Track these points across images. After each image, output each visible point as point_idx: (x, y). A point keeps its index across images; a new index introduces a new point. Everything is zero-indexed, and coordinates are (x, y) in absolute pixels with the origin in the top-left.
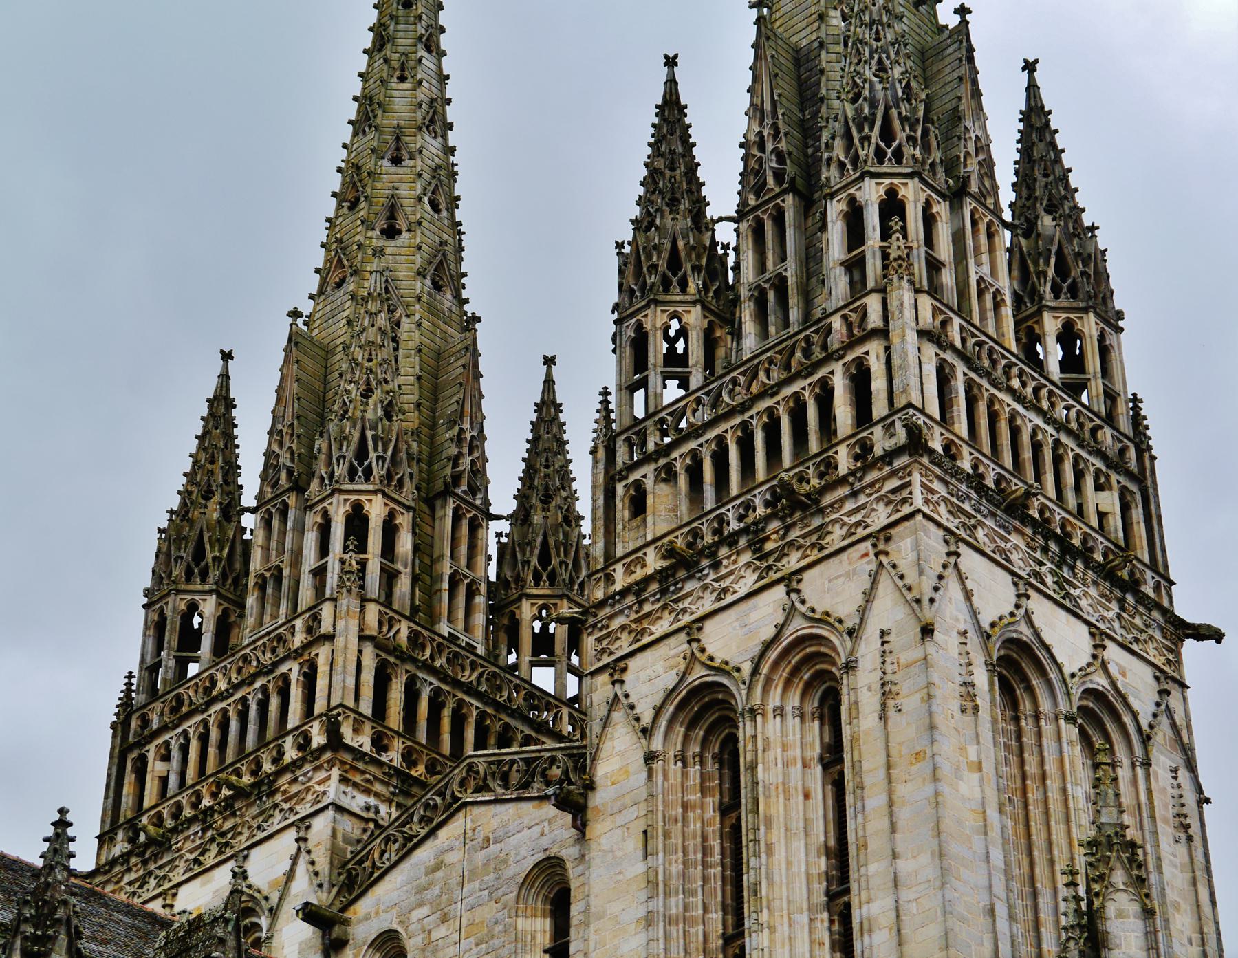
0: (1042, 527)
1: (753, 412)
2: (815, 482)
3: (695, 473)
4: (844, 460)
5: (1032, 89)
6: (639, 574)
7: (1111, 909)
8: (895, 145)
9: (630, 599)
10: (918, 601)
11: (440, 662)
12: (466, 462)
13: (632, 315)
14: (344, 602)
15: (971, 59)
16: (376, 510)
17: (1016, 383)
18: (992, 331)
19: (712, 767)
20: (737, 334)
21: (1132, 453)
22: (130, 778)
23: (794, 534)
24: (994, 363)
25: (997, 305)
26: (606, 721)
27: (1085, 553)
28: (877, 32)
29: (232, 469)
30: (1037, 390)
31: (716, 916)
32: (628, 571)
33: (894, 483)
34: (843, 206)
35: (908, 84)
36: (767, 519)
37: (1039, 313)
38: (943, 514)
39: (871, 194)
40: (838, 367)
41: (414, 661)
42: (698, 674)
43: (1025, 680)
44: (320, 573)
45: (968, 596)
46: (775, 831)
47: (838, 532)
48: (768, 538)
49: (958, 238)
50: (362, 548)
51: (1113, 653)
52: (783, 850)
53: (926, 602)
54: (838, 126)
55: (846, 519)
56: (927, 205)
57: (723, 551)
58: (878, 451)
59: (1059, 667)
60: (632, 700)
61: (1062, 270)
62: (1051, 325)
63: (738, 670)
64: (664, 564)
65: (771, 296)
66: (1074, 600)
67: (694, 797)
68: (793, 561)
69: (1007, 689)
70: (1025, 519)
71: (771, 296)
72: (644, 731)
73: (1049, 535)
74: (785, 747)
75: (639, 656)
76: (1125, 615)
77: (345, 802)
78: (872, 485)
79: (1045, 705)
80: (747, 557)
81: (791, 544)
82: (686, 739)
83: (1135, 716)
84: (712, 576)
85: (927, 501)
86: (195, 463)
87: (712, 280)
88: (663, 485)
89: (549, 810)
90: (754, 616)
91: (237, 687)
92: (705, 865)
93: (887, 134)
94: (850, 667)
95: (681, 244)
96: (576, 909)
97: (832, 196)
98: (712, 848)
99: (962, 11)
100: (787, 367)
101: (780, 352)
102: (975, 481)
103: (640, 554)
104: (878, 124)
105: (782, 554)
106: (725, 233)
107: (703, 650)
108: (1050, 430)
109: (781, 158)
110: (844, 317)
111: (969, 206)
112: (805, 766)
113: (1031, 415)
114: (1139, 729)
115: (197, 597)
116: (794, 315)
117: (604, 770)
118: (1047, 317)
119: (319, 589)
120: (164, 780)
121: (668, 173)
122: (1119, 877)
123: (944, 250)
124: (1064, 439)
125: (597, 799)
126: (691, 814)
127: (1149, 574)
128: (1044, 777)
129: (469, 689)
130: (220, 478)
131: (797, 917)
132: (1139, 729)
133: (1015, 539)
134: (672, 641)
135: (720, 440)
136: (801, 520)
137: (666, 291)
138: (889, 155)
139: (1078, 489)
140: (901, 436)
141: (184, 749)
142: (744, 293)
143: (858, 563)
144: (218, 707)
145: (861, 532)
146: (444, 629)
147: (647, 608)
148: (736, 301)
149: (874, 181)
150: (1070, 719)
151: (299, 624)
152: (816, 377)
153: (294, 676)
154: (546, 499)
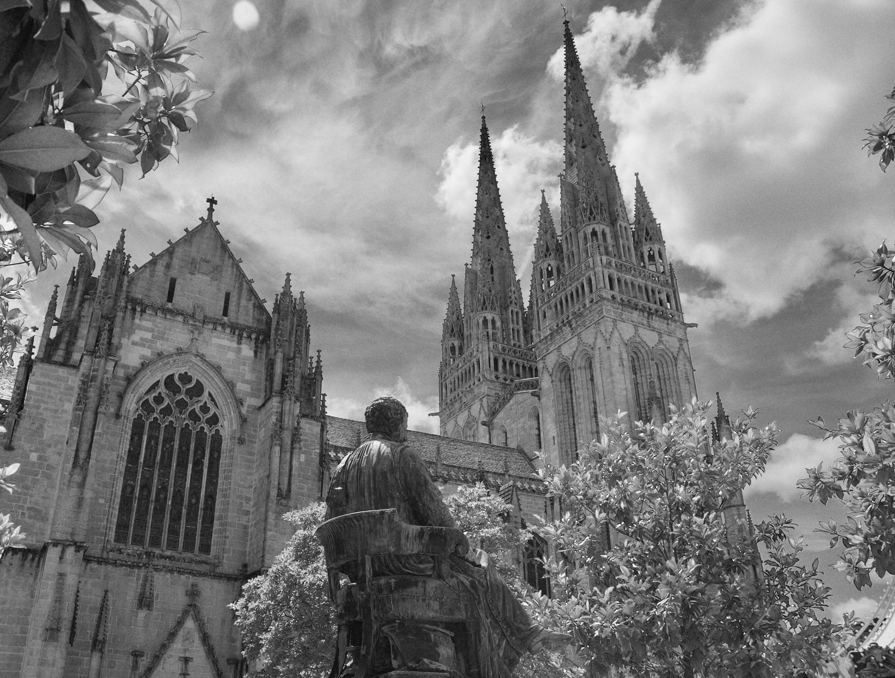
3: (556, 307)
4: (587, 302)
5: (638, 181)
9: (544, 341)
15: (617, 180)
19: (567, 382)
22: (444, 388)
39: (589, 230)
42: (560, 360)
47: (588, 322)
51: (665, 338)
61: (647, 234)
65: (571, 256)
68: (579, 330)
71: (571, 256)
93: (591, 213)
102: (622, 303)
104: (589, 210)
114: (674, 357)
122: (655, 406)
127: (676, 312)
132: (674, 357)
143: (592, 330)
146: (512, 342)
147: (549, 343)
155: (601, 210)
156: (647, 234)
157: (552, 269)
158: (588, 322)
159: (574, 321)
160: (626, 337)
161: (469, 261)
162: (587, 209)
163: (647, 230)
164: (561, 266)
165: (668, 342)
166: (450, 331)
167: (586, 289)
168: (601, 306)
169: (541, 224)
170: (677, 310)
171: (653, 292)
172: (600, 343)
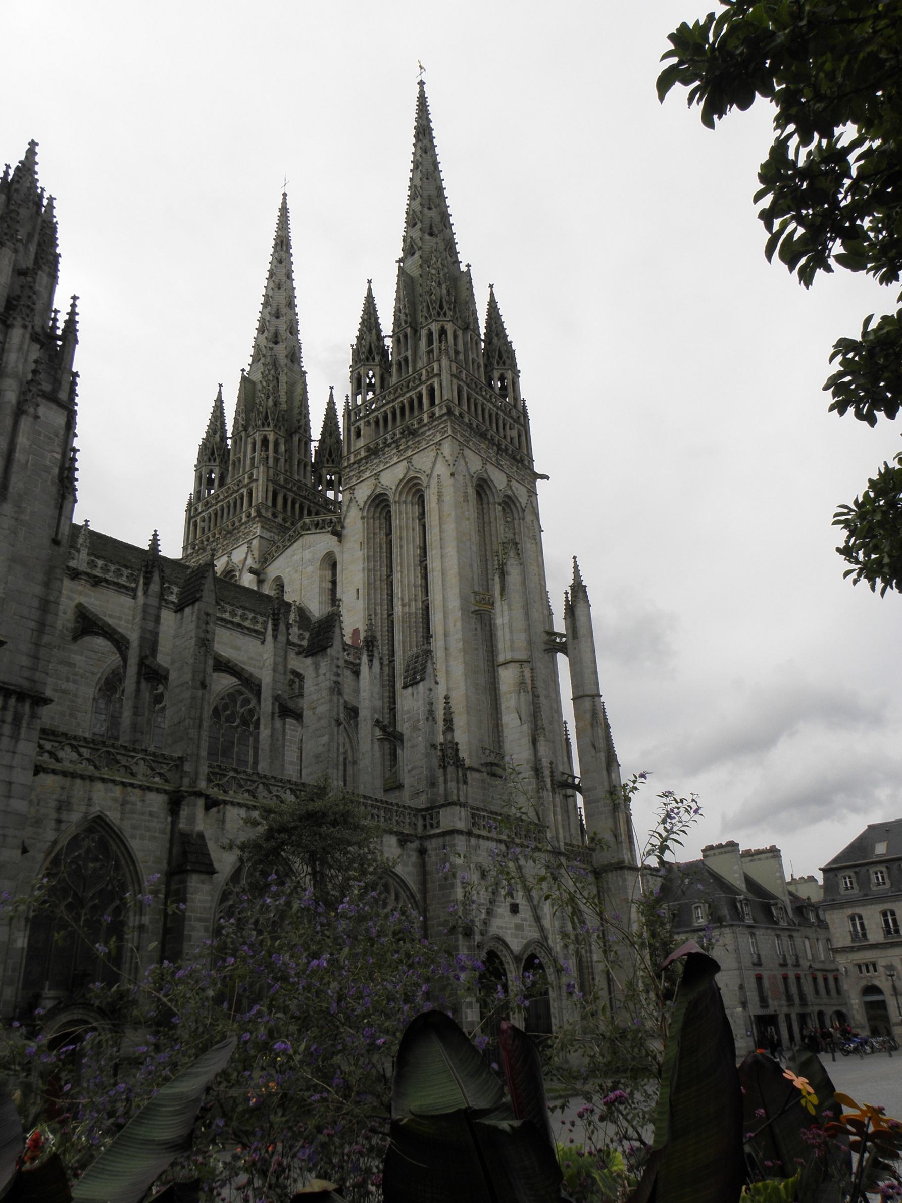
0: (492, 441)
2: (416, 426)
6: (359, 457)
7: (509, 563)
9: (356, 466)
11: (295, 488)
12: (303, 422)
14: (261, 468)
15: (471, 283)
16: (271, 437)
17: (484, 393)
18: (477, 376)
19: (383, 521)
20: (391, 376)
21: (522, 418)
23: (410, 443)
24: (476, 386)
25: (479, 367)
26: (349, 506)
27: (506, 450)
29: (223, 424)
30: (491, 396)
31: (384, 569)
32: (355, 456)
33: (442, 426)
36: (400, 438)
38: (458, 436)
39: (435, 328)
40: (424, 387)
41: (286, 488)
42: (378, 491)
43: (485, 492)
44: (253, 459)
45: (466, 463)
49: (465, 344)
50: (267, 450)
51: (514, 484)
54: (425, 304)
56: (455, 332)
57: (387, 449)
58: (437, 415)
59: (496, 487)
61: (500, 356)
62: (496, 375)
64: (366, 454)
65: (403, 363)
66: (501, 466)
68: (409, 453)
69: (478, 493)
70: (486, 438)
71: (403, 363)
73: (494, 444)
74: (406, 514)
77: (264, 535)
79: (491, 500)
80: (395, 451)
82: (374, 512)
83: (520, 503)
85: (453, 432)
89: (330, 536)
90: (396, 471)
91: (226, 497)
94: (428, 486)
96: (339, 567)
97: (423, 328)
99: (468, 266)
100: (408, 386)
102: (470, 426)
105: (406, 450)
106: (388, 342)
108: (495, 409)
109: (406, 315)
111: (469, 333)
112: (413, 520)
113: (489, 405)
116: (410, 369)
117: (348, 522)
118: (495, 372)
119: (253, 464)
120: (203, 529)
122: (512, 554)
123: (461, 348)
124: (500, 412)
125: (345, 532)
128: (490, 523)
129: (304, 498)
133: (483, 445)
135: (385, 412)
139: (504, 429)
140: (445, 410)
141: (210, 518)
142: (394, 362)
144: (220, 504)
145: (432, 443)
148: (391, 365)
150: (499, 504)
151: (246, 476)
153: (245, 493)
154: (331, 435)
156: (500, 356)
160: (472, 470)
161: (248, 369)
165: (517, 489)
166: (208, 452)
167: (425, 401)
172: (441, 469)
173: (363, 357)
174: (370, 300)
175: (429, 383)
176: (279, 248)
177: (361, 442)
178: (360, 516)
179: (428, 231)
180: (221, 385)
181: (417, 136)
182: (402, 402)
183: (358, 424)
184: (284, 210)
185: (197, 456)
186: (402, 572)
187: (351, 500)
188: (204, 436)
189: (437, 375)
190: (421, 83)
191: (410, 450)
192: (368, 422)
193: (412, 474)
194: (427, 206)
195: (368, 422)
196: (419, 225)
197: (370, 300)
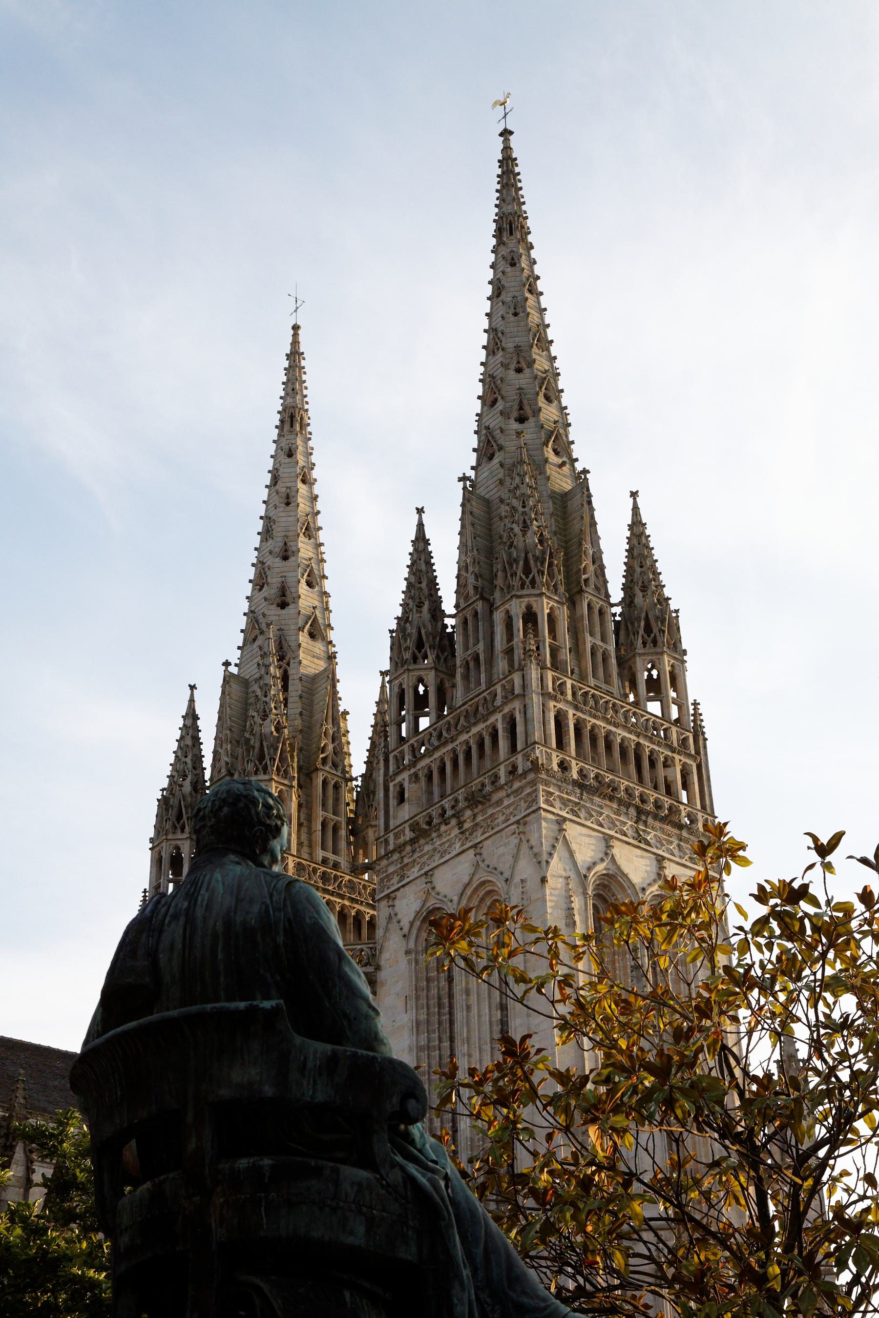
1: (457, 742)
3: (429, 777)
4: (502, 772)
5: (636, 509)
6: (402, 840)
8: (531, 576)
9: (396, 856)
10: (540, 863)
13: (396, 678)
15: (590, 503)
23: (479, 818)
26: (387, 930)
28: (524, 502)
29: (199, 758)
32: (397, 836)
34: (503, 615)
35: (541, 535)
37: (634, 656)
39: (517, 608)
40: (498, 716)
42: (431, 903)
45: (571, 854)
46: (471, 997)
48: (465, 821)
52: (476, 1008)
53: (544, 864)
55: (504, 811)
57: (443, 828)
60: (399, 916)
61: (648, 629)
63: (451, 901)
64: (412, 835)
65: (472, 664)
67: (433, 974)
71: (472, 664)
72: (405, 936)
75: (402, 890)
76: (682, 843)
78: (516, 791)
81: (477, 824)
84: (438, 843)
86: (176, 757)
87: (443, 653)
88: (413, 785)
92: (439, 1014)
93: (527, 570)
95: (423, 632)
98: (444, 1004)
101: (471, 706)
103: (401, 828)
104: (521, 563)
107: (434, 888)
108: (633, 737)
110: (503, 686)
115: (179, 843)
117: (385, 958)
118: (638, 658)
121: (418, 585)
124: (642, 741)
126: (432, 985)
127: (700, 814)
130: (190, 766)
131: (484, 1047)
134: (418, 881)
136: (482, 811)
137: (415, 662)
138: (528, 583)
145: (513, 820)
146: (320, 854)
147: (406, 861)
149: (519, 600)
152: (488, 723)
155: (550, 565)
157: (426, 691)
158: (501, 818)
159: (468, 813)
161: (234, 656)
162: (516, 561)
163: (647, 618)
164: (447, 685)
166: (172, 814)
168: (533, 783)
169: (410, 586)
170: (703, 807)
171: (652, 763)
173: (407, 655)
174: (421, 542)
175: (506, 710)
176: (287, 427)
177: (405, 813)
178: (404, 949)
179: (515, 414)
180: (192, 687)
181: (499, 234)
182: (467, 742)
183: (399, 779)
184: (295, 355)
185: (153, 821)
186: (470, 1056)
187: (390, 918)
188: (165, 783)
189: (517, 696)
190: (506, 133)
191: (480, 831)
192: (416, 775)
193: (482, 876)
194: (513, 366)
195: (416, 775)
196: (500, 405)
197: (421, 542)
